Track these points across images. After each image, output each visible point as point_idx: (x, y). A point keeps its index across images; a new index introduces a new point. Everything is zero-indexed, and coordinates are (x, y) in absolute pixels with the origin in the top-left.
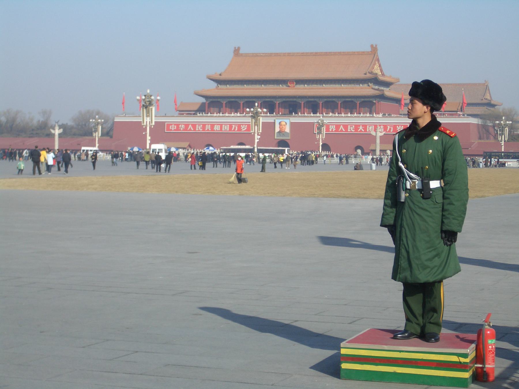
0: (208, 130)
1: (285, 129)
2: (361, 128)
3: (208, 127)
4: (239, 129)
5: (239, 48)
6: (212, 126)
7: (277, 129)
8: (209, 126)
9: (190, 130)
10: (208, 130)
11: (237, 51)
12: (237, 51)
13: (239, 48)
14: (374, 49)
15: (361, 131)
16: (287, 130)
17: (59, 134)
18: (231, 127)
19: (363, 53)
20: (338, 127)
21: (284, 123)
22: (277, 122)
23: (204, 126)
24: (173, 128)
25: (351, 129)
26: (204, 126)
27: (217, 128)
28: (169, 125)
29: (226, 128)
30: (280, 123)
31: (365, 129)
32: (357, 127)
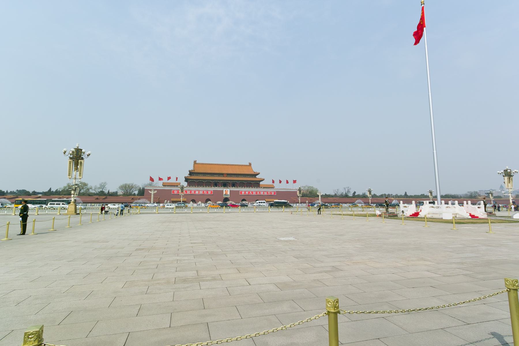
3: (193, 192)
4: (207, 192)
6: (195, 192)
7: (224, 193)
11: (195, 162)
12: (195, 162)
14: (250, 164)
16: (229, 193)
17: (154, 194)
18: (203, 192)
19: (246, 166)
20: (249, 192)
22: (224, 190)
24: (176, 192)
25: (254, 193)
27: (197, 192)
28: (173, 191)
29: (201, 192)
32: (256, 193)
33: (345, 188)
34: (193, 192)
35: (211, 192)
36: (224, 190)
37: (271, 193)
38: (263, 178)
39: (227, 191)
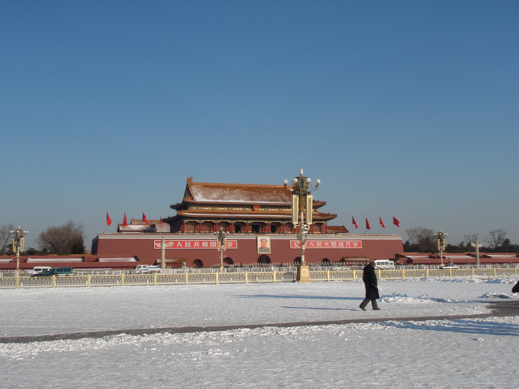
0: (197, 247)
1: (266, 245)
2: (326, 244)
3: (197, 244)
5: (191, 178)
6: (201, 243)
7: (259, 246)
8: (198, 243)
9: (179, 246)
10: (197, 247)
13: (191, 178)
15: (327, 246)
16: (268, 245)
21: (265, 240)
23: (192, 243)
26: (192, 243)
30: (261, 240)
31: (330, 245)
33: (493, 233)
34: (197, 244)
35: (234, 243)
36: (260, 238)
37: (352, 244)
38: (332, 213)
39: (265, 242)
